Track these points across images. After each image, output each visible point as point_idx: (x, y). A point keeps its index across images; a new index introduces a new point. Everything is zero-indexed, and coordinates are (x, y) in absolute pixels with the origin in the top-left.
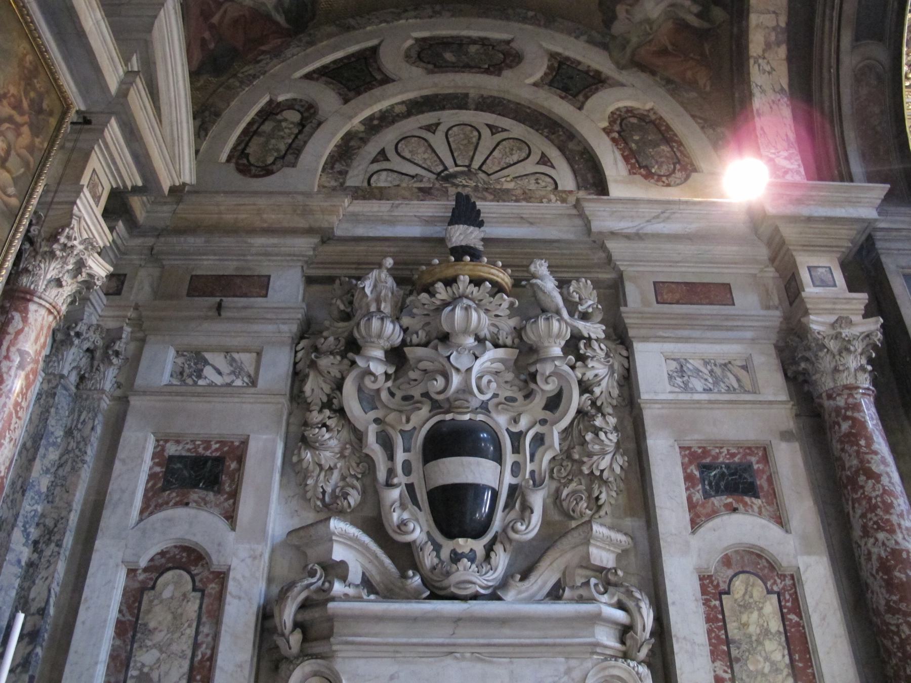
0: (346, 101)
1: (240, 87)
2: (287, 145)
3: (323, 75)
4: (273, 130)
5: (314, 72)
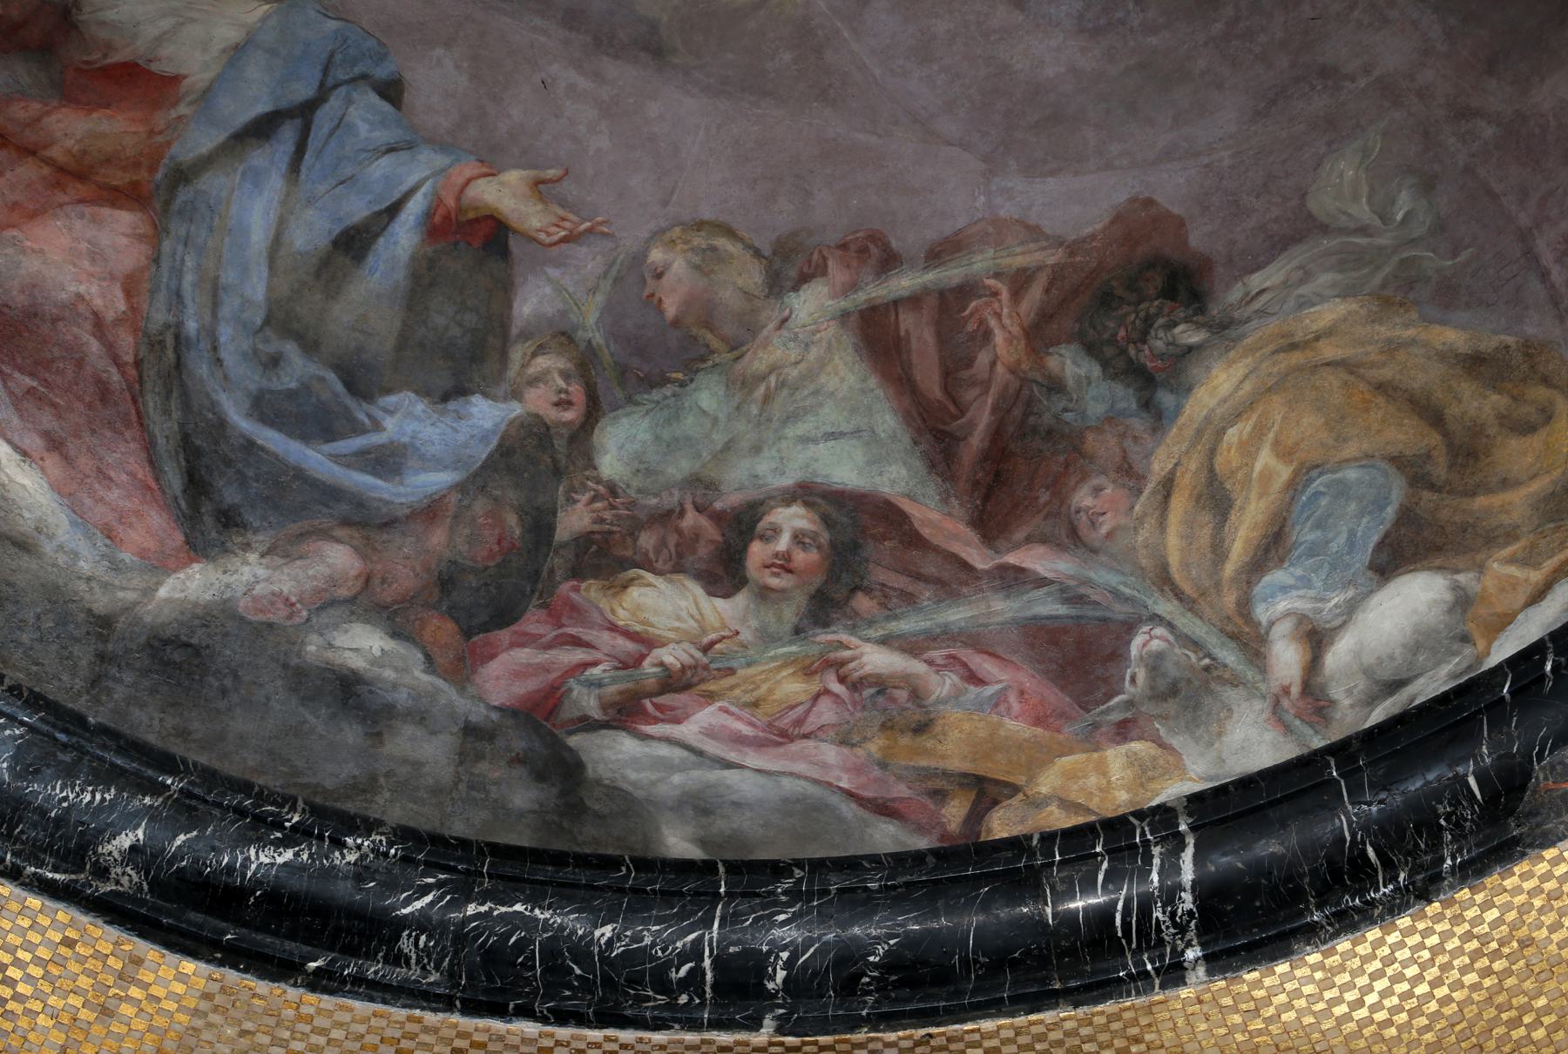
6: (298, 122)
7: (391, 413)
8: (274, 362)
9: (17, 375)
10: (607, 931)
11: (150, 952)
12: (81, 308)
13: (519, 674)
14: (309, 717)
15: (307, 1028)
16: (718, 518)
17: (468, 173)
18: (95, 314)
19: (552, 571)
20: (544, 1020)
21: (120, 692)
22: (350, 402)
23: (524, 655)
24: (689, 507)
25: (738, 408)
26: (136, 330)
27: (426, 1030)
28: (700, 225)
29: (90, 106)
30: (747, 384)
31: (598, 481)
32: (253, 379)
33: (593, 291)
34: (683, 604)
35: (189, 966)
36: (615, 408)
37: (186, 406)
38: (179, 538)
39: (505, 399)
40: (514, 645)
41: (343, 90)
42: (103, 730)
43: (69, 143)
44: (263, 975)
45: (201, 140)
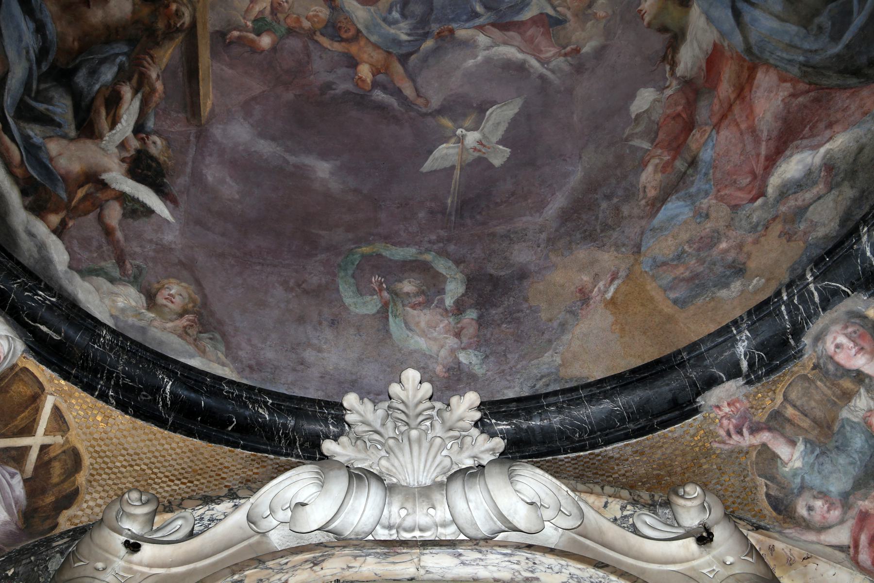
8: (820, 28)
9: (804, 132)
12: (787, 101)
18: (790, 96)
29: (719, 80)
43: (730, 91)
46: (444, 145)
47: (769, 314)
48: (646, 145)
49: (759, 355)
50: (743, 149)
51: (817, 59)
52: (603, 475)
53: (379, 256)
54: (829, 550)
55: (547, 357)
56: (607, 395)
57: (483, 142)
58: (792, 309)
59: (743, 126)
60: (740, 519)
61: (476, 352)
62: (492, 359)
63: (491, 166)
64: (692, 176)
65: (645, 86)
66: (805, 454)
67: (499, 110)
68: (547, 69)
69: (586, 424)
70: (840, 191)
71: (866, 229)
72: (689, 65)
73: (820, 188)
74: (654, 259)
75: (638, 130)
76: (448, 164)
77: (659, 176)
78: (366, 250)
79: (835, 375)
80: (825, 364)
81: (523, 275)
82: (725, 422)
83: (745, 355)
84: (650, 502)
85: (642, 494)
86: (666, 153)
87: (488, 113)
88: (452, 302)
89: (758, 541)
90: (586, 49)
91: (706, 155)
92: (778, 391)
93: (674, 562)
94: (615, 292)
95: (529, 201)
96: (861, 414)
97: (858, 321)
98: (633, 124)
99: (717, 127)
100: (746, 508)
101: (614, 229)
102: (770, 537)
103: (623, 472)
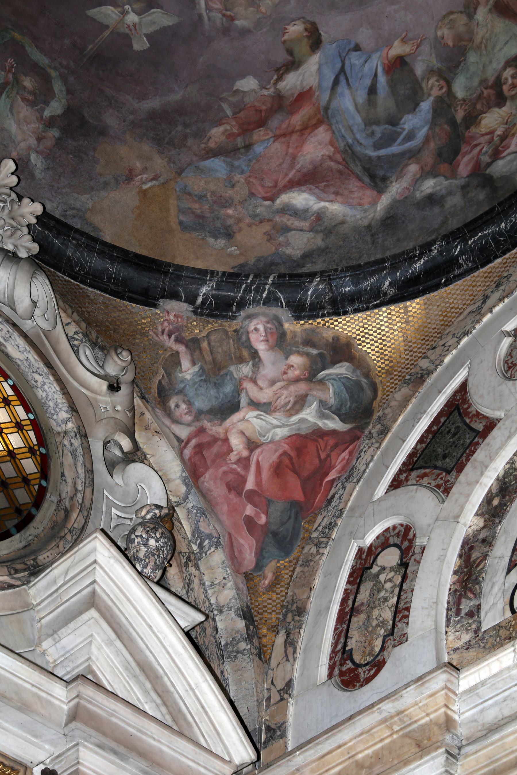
0: (447, 491)
1: (318, 553)
2: (393, 609)
3: (412, 470)
4: (371, 595)
5: (400, 471)
6: (342, 74)
7: (404, 124)
8: (373, 133)
10: (503, 225)
11: (408, 303)
12: (324, 158)
13: (467, 165)
14: (426, 213)
15: (451, 295)
16: (491, 87)
17: (386, 52)
19: (462, 132)
20: (501, 256)
21: (380, 241)
22: (395, 129)
23: (466, 159)
24: (484, 90)
25: (481, 55)
26: (339, 153)
27: (476, 277)
28: (444, 17)
30: (479, 47)
31: (460, 101)
32: (370, 142)
33: (431, 55)
34: (495, 116)
35: (417, 300)
36: (453, 79)
37: (360, 160)
38: (375, 193)
39: (428, 98)
40: (462, 158)
41: (347, 58)
42: (366, 264)
43: (299, 123)
44: (434, 291)
45: (325, 97)
46: (112, 8)
47: (234, 283)
48: (229, 113)
49: (211, 300)
50: (281, 164)
51: (358, 149)
52: (77, 304)
53: (23, 47)
54: (172, 436)
55: (84, 198)
56: (111, 258)
57: (137, 27)
58: (249, 290)
59: (291, 151)
60: (137, 386)
61: (43, 161)
62: (51, 172)
63: (131, 46)
64: (242, 155)
65: (255, 76)
66: (196, 374)
67: (160, 14)
68: (207, 14)
69: (87, 265)
70: (315, 236)
71: (319, 279)
72: (288, 87)
73: (305, 225)
74: (186, 186)
75: (231, 99)
76: (105, 22)
77: (223, 138)
78: (17, 36)
79: (243, 344)
80: (242, 333)
81: (103, 132)
82: (166, 324)
83: (204, 295)
84: (94, 341)
85: (92, 332)
86: (237, 128)
87: (153, 10)
88: (49, 115)
89: (138, 405)
90: (237, 22)
91: (259, 149)
92: (206, 328)
93: (88, 389)
94: (150, 188)
95: (138, 88)
96: (241, 375)
97: (276, 324)
98: (231, 93)
99: (277, 137)
100: (143, 381)
101: (175, 148)
102: (146, 408)
103: (89, 310)
